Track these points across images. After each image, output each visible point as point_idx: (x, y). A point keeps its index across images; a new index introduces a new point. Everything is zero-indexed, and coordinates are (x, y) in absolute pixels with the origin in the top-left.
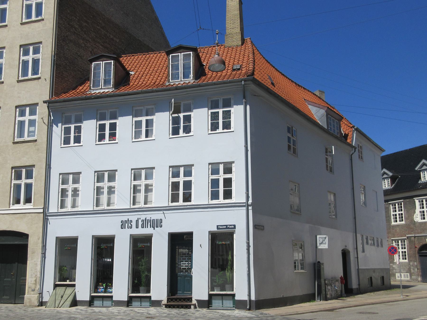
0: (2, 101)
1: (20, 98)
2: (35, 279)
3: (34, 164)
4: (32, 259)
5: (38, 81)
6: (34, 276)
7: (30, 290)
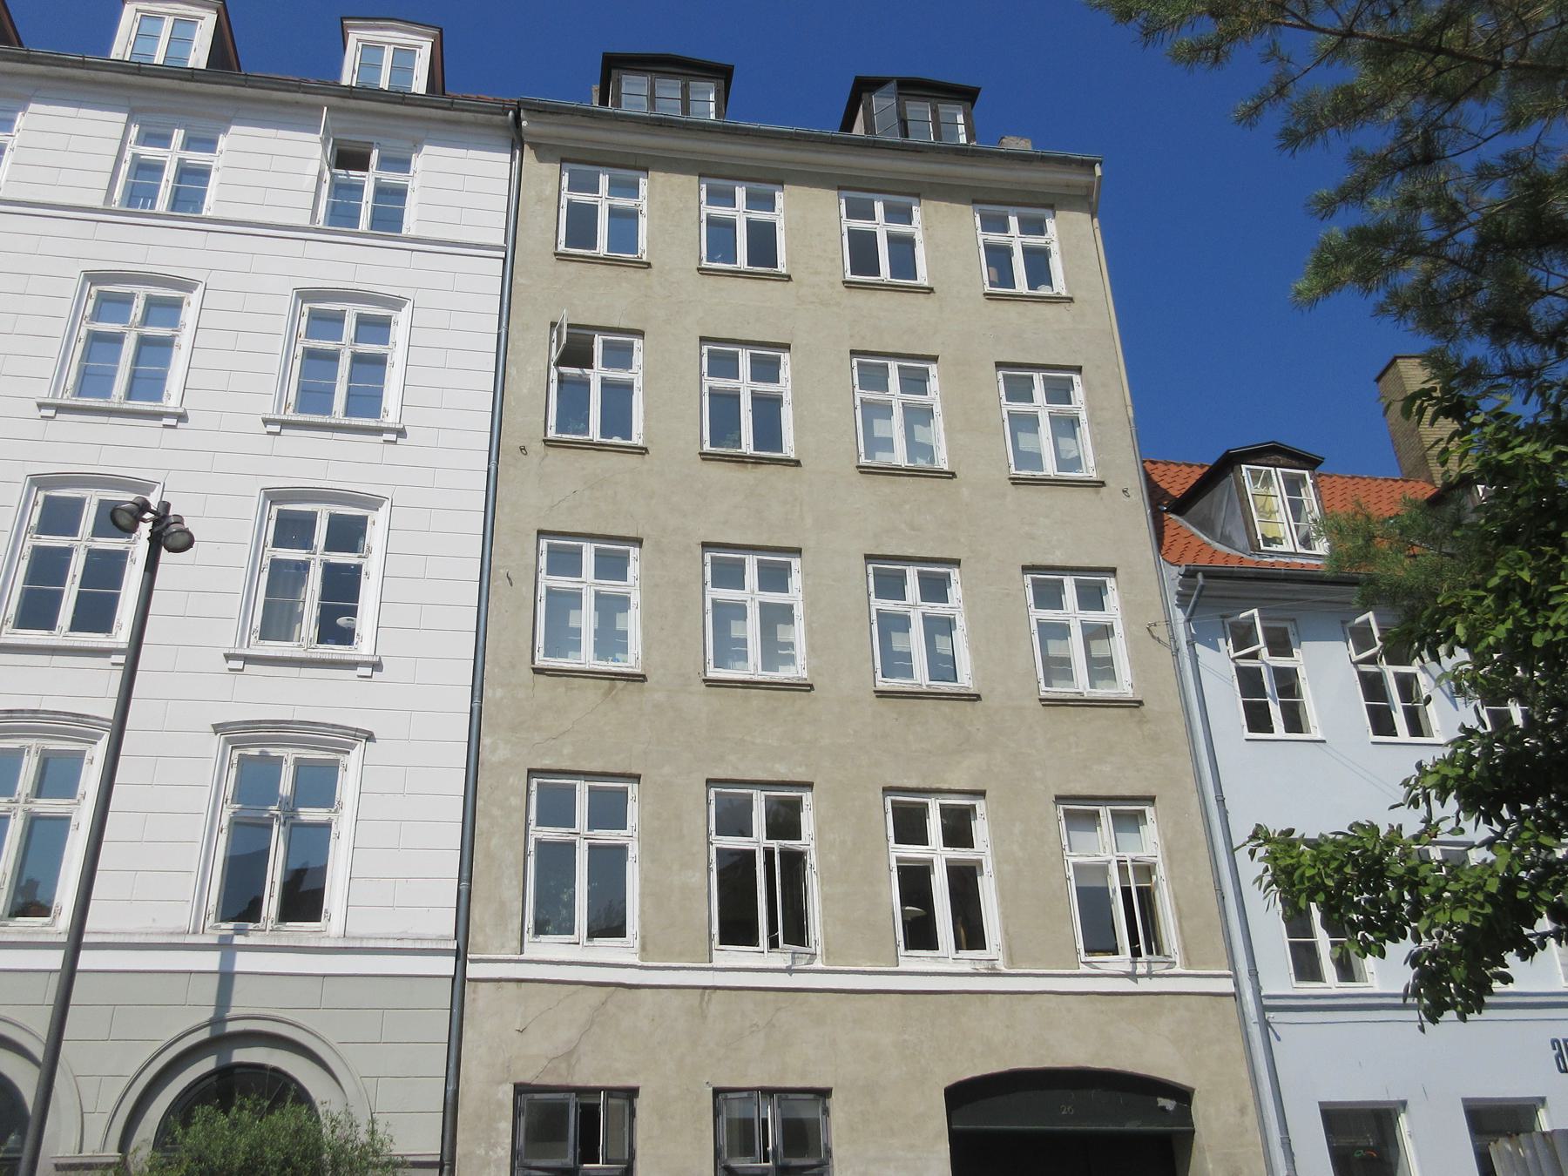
0: (962, 540)
1: (1033, 538)
3: (1152, 791)
5: (1098, 493)
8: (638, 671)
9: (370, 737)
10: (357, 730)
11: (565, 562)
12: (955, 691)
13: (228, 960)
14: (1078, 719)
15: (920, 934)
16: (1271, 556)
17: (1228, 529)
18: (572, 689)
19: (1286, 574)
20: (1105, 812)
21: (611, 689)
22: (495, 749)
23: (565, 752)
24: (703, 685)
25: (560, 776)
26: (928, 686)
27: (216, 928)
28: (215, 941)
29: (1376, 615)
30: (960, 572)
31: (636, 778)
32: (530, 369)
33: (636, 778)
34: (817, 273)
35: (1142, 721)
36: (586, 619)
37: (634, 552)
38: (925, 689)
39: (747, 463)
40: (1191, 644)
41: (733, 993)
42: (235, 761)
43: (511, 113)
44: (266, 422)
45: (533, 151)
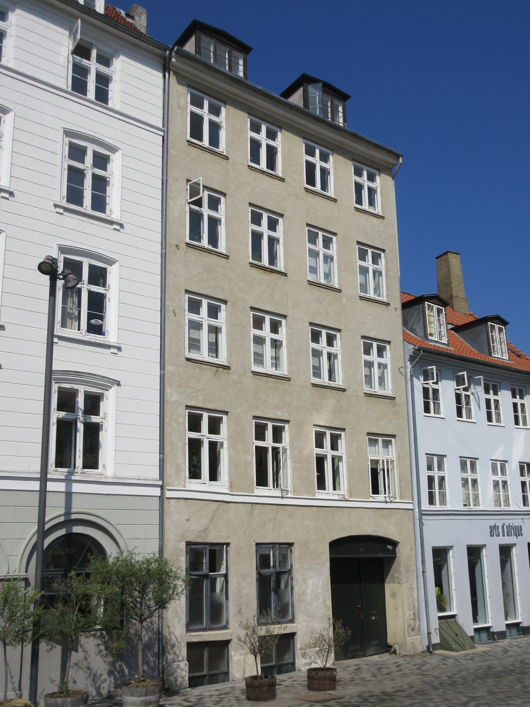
1: (365, 324)
2: (412, 612)
4: (407, 582)
6: (412, 607)
7: (410, 630)
8: (225, 364)
9: (118, 384)
10: (114, 380)
11: (194, 307)
12: (334, 386)
13: (69, 487)
14: (376, 403)
15: (321, 485)
16: (431, 342)
17: (415, 327)
18: (202, 370)
19: (446, 354)
20: (380, 439)
21: (217, 371)
22: (172, 395)
23: (200, 399)
24: (251, 374)
25: (197, 409)
26: (328, 383)
27: (56, 471)
28: (64, 478)
29: (467, 373)
30: (341, 335)
31: (226, 413)
32: (178, 203)
33: (226, 413)
34: (294, 180)
35: (394, 406)
36: (204, 336)
37: (223, 306)
38: (327, 384)
39: (267, 271)
40: (411, 377)
41: (262, 505)
42: (57, 390)
43: (168, 52)
44: (56, 206)
45: (175, 77)
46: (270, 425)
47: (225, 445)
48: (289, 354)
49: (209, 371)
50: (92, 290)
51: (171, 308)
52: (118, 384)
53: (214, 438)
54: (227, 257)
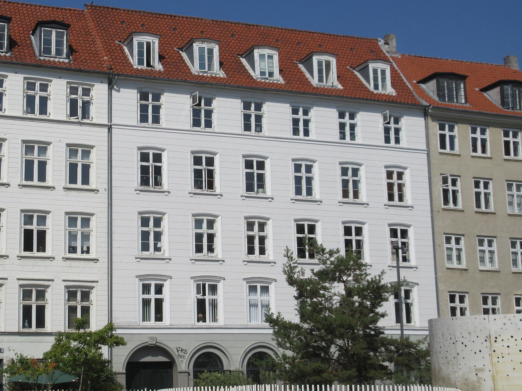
9: (418, 284)
21: (462, 272)
22: (441, 287)
31: (467, 293)
46: (490, 297)
47: (468, 309)
48: (499, 258)
49: (458, 273)
50: (403, 241)
51: (438, 244)
52: (418, 284)
53: (462, 305)
54: (463, 211)
